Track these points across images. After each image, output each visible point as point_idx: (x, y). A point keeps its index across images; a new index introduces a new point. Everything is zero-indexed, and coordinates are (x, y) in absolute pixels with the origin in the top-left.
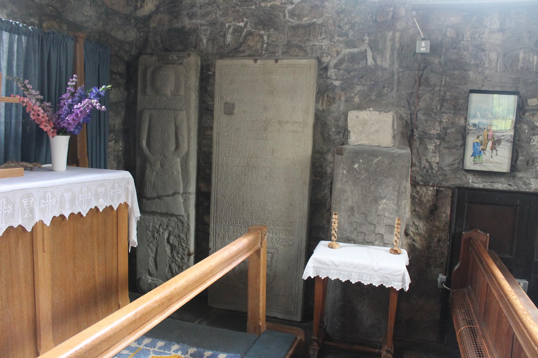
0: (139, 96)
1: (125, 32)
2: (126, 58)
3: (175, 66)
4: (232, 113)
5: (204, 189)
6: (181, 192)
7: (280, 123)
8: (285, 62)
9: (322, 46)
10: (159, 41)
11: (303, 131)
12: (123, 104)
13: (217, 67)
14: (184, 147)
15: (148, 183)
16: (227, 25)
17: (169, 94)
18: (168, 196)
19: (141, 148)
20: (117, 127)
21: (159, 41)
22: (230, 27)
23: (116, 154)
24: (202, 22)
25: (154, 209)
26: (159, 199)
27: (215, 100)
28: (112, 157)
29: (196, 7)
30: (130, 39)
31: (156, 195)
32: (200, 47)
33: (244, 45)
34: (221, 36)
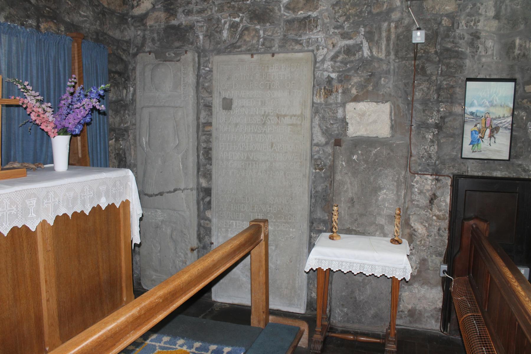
1: (122, 32)
7: (278, 118)
8: (281, 55)
9: (318, 39)
10: (156, 38)
11: (301, 124)
16: (223, 21)
18: (170, 192)
21: (156, 38)
22: (225, 23)
28: (113, 155)
29: (191, 3)
30: (127, 38)
32: (197, 43)
33: (240, 40)
34: (217, 32)
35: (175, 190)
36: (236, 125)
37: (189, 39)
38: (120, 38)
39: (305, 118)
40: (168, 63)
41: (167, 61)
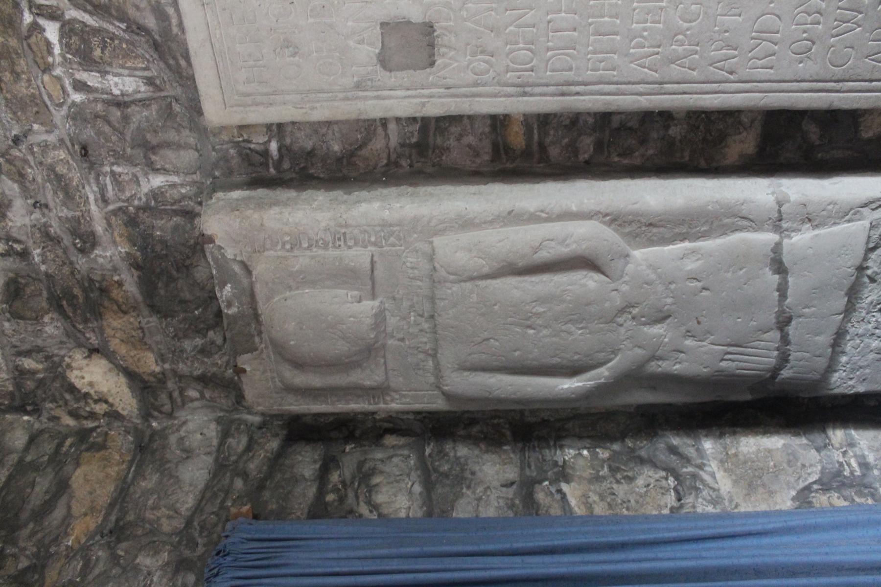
0: (395, 406)
1: (188, 453)
2: (274, 444)
3: (258, 288)
4: (428, 29)
5: (743, 144)
6: (769, 237)
10: (199, 341)
12: (428, 451)
13: (236, 118)
14: (584, 235)
15: (723, 364)
17: (369, 306)
18: (782, 290)
19: (588, 395)
20: (511, 473)
21: (199, 341)
22: (79, 86)
23: (605, 471)
24: (92, 197)
25: (824, 340)
26: (789, 320)
27: (377, 114)
28: (621, 490)
29: (46, 226)
30: (213, 431)
31: (776, 335)
32: (184, 197)
34: (126, 119)
35: (779, 267)
37: (176, 228)
38: (210, 460)
40: (262, 308)
41: (255, 309)
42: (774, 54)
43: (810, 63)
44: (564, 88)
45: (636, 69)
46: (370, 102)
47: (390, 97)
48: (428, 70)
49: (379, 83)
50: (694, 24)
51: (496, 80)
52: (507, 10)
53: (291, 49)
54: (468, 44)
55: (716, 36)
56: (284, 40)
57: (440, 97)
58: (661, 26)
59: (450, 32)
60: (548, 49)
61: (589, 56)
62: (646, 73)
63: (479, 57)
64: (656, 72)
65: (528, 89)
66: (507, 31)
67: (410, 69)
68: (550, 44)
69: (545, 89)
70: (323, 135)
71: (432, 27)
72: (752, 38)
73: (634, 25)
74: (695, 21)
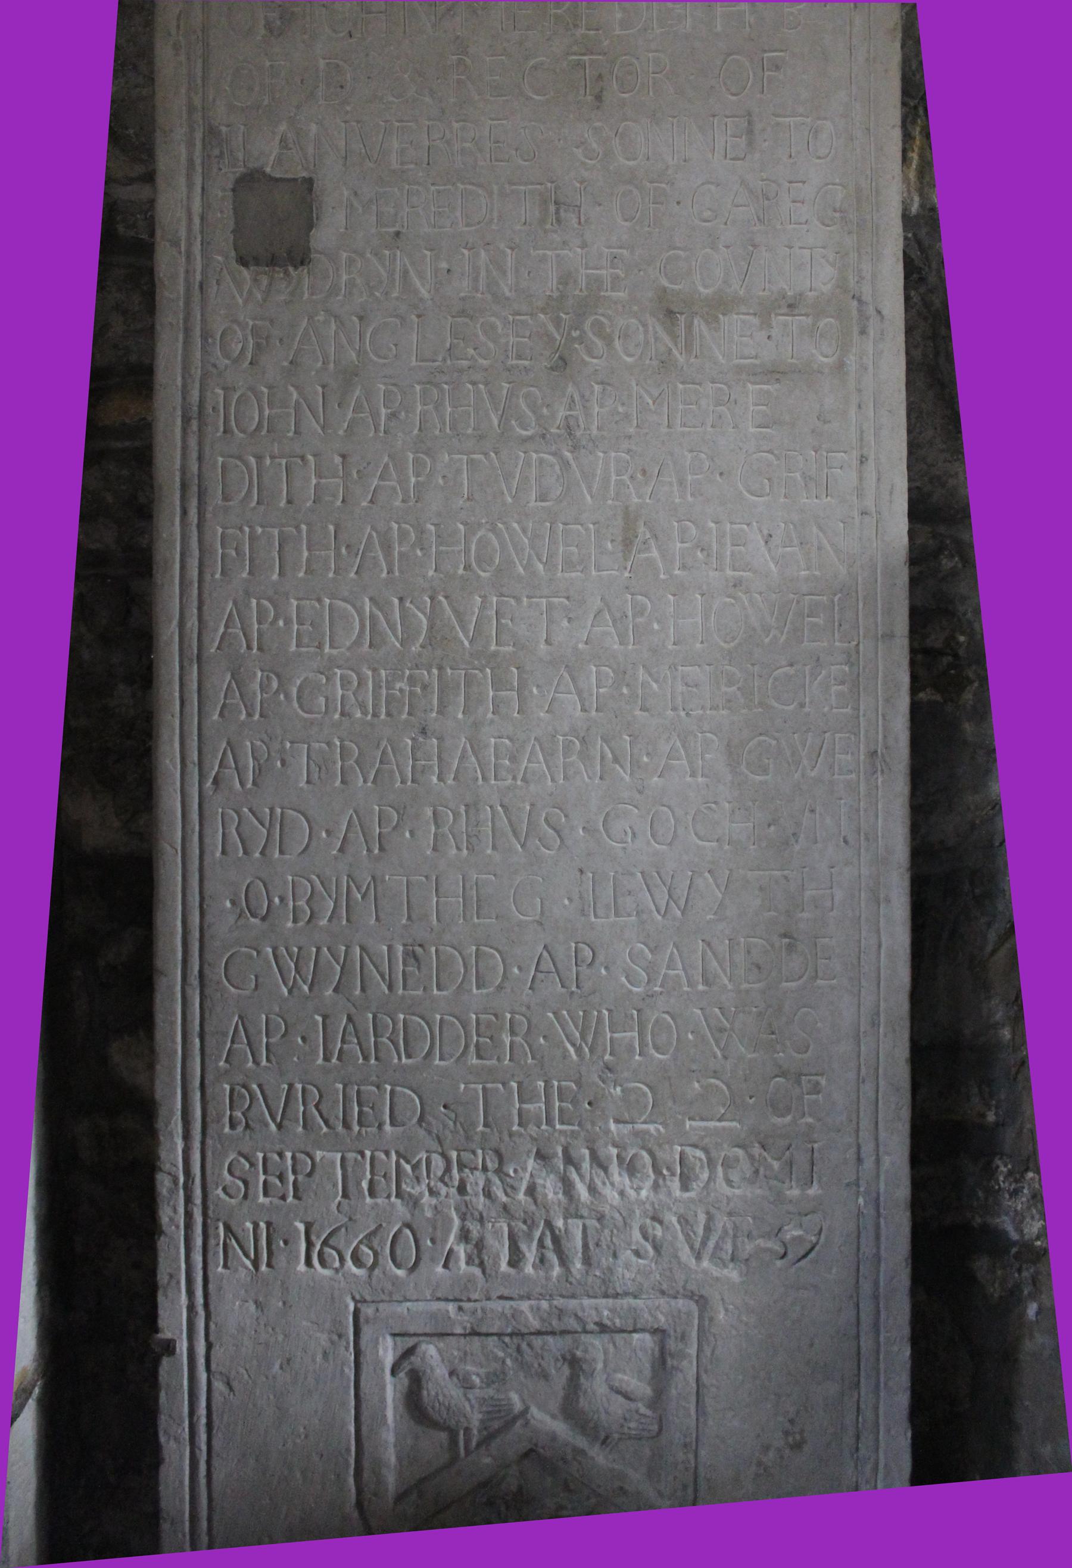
4: (299, 257)
11: (841, 366)
36: (349, 376)
39: (863, 317)
42: (245, 852)
43: (231, 919)
44: (195, 489)
45: (224, 609)
46: (184, 151)
47: (190, 186)
48: (233, 254)
49: (215, 170)
50: (296, 705)
51: (211, 369)
52: (323, 387)
53: (278, 23)
54: (272, 321)
55: (276, 746)
56: (293, 13)
57: (187, 272)
58: (293, 648)
59: (292, 294)
60: (259, 458)
61: (247, 529)
62: (216, 630)
63: (250, 338)
64: (218, 648)
65: (194, 424)
66: (292, 389)
67: (236, 223)
68: (268, 461)
69: (194, 455)
70: (135, 67)
71: (302, 263)
72: (272, 810)
73: (295, 603)
74: (301, 707)
